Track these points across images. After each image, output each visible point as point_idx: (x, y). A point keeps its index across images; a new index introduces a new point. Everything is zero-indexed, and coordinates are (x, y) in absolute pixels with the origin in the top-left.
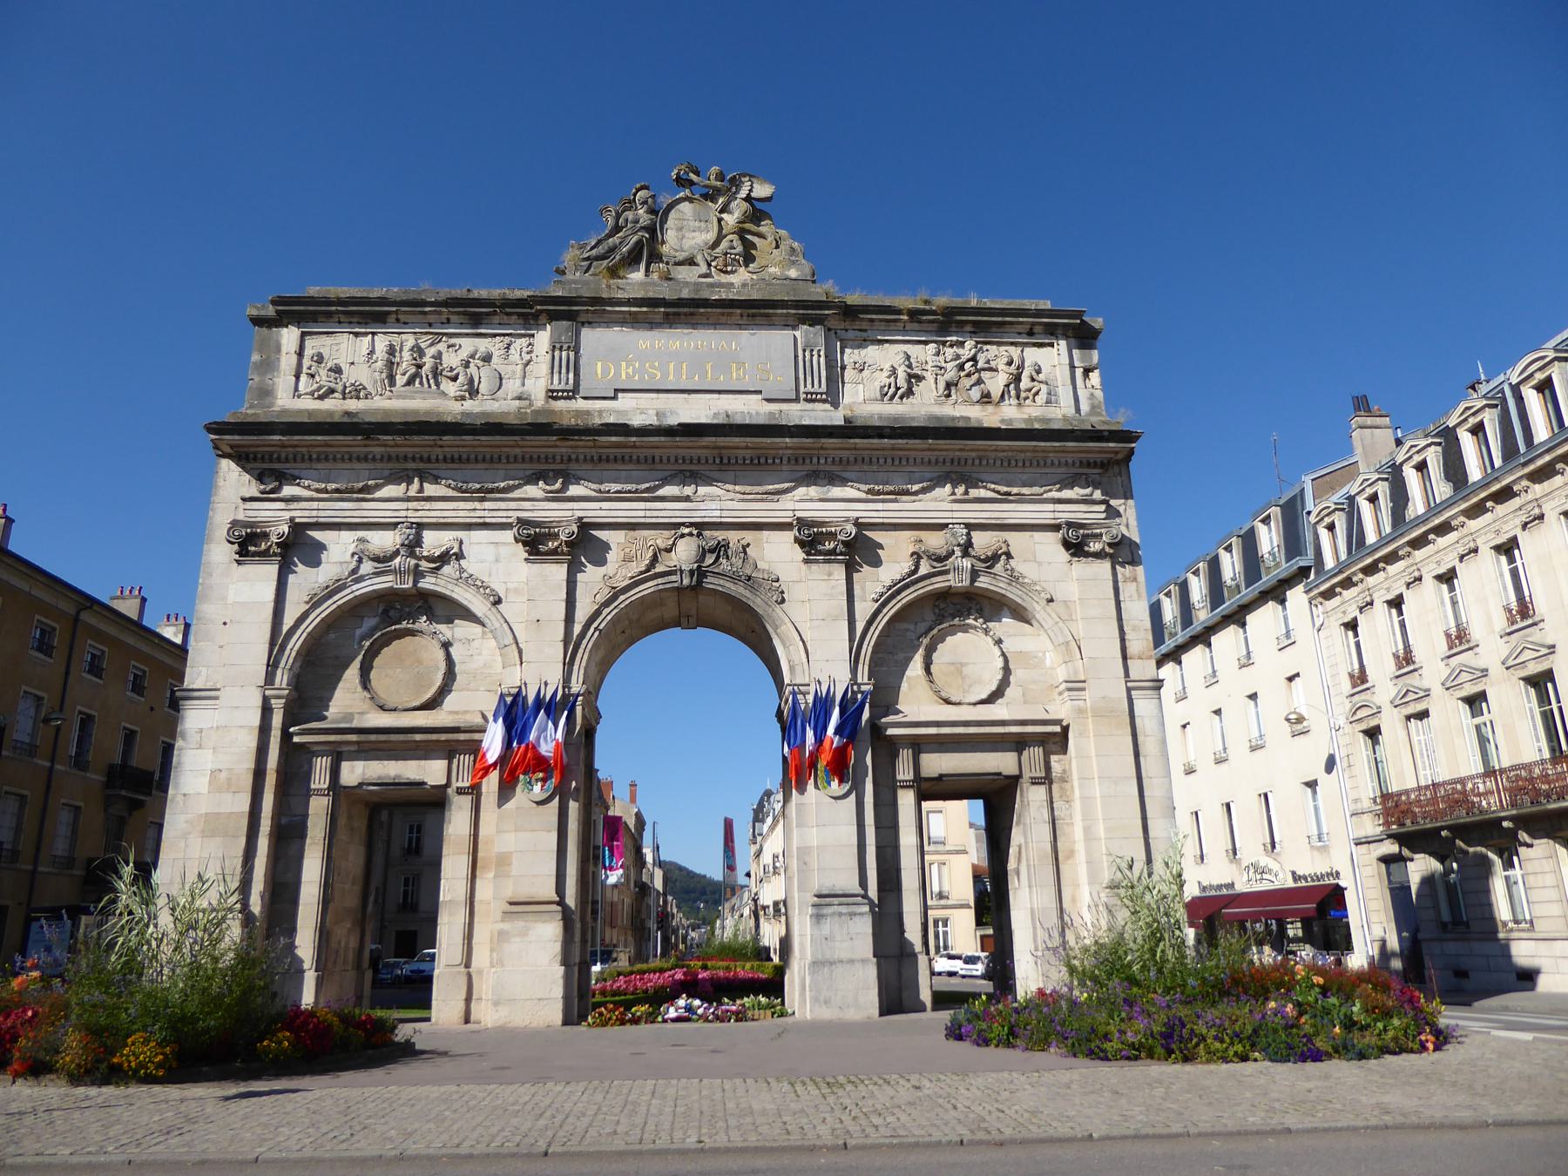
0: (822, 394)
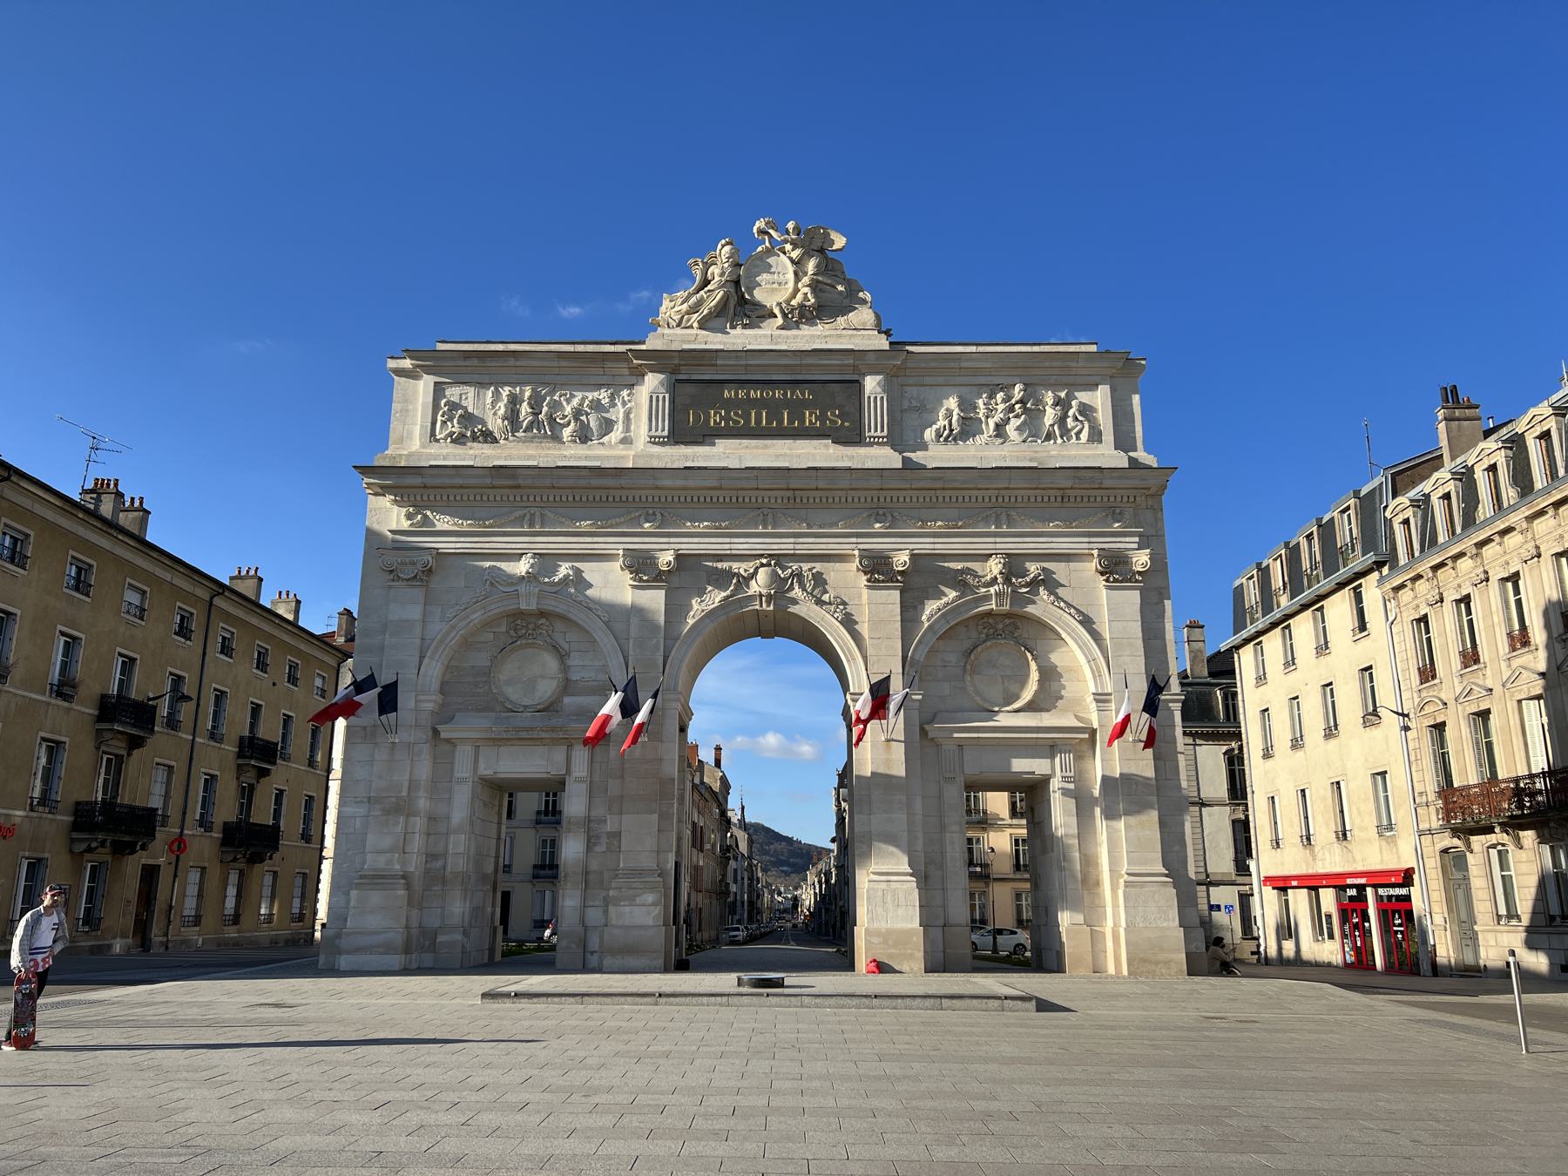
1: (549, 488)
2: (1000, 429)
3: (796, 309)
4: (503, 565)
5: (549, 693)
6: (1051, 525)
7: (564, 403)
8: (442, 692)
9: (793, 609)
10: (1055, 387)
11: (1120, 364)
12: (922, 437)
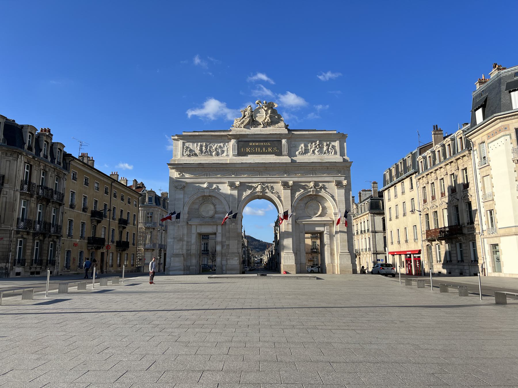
0: (286, 154)
1: (211, 167)
7: (213, 146)
8: (188, 214)
9: (266, 194)
10: (326, 141)
11: (341, 136)
12: (296, 154)
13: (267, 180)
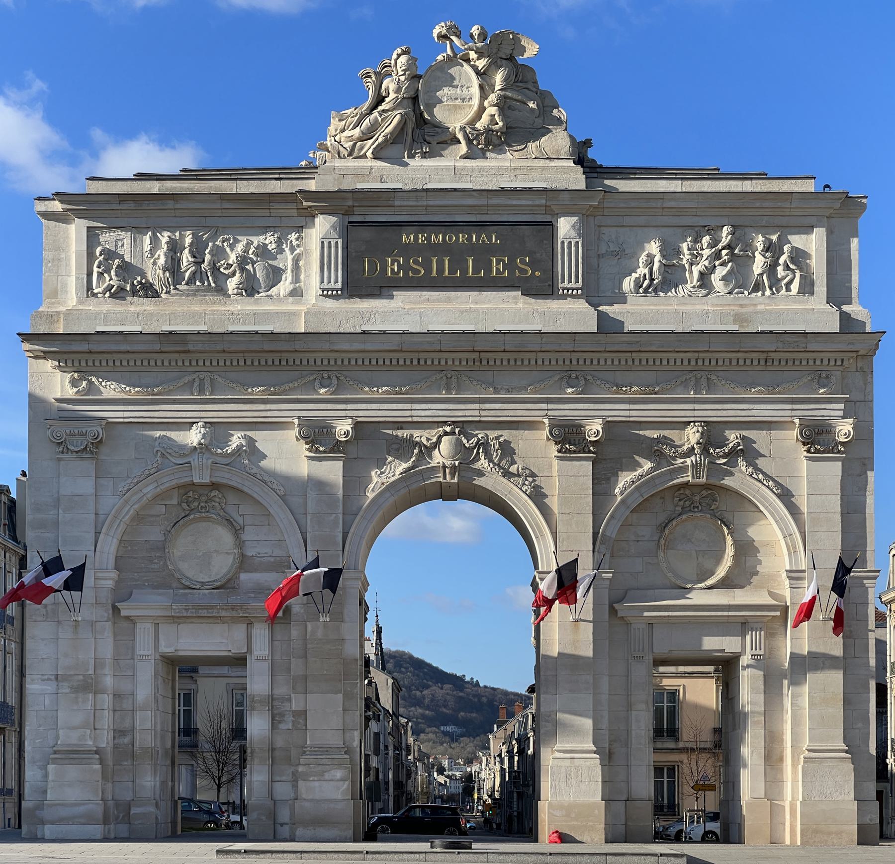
1: (218, 352)
2: (704, 277)
3: (482, 134)
4: (173, 435)
5: (225, 570)
6: (753, 390)
7: (228, 249)
8: (117, 568)
10: (765, 229)
11: (838, 205)
13: (484, 413)
